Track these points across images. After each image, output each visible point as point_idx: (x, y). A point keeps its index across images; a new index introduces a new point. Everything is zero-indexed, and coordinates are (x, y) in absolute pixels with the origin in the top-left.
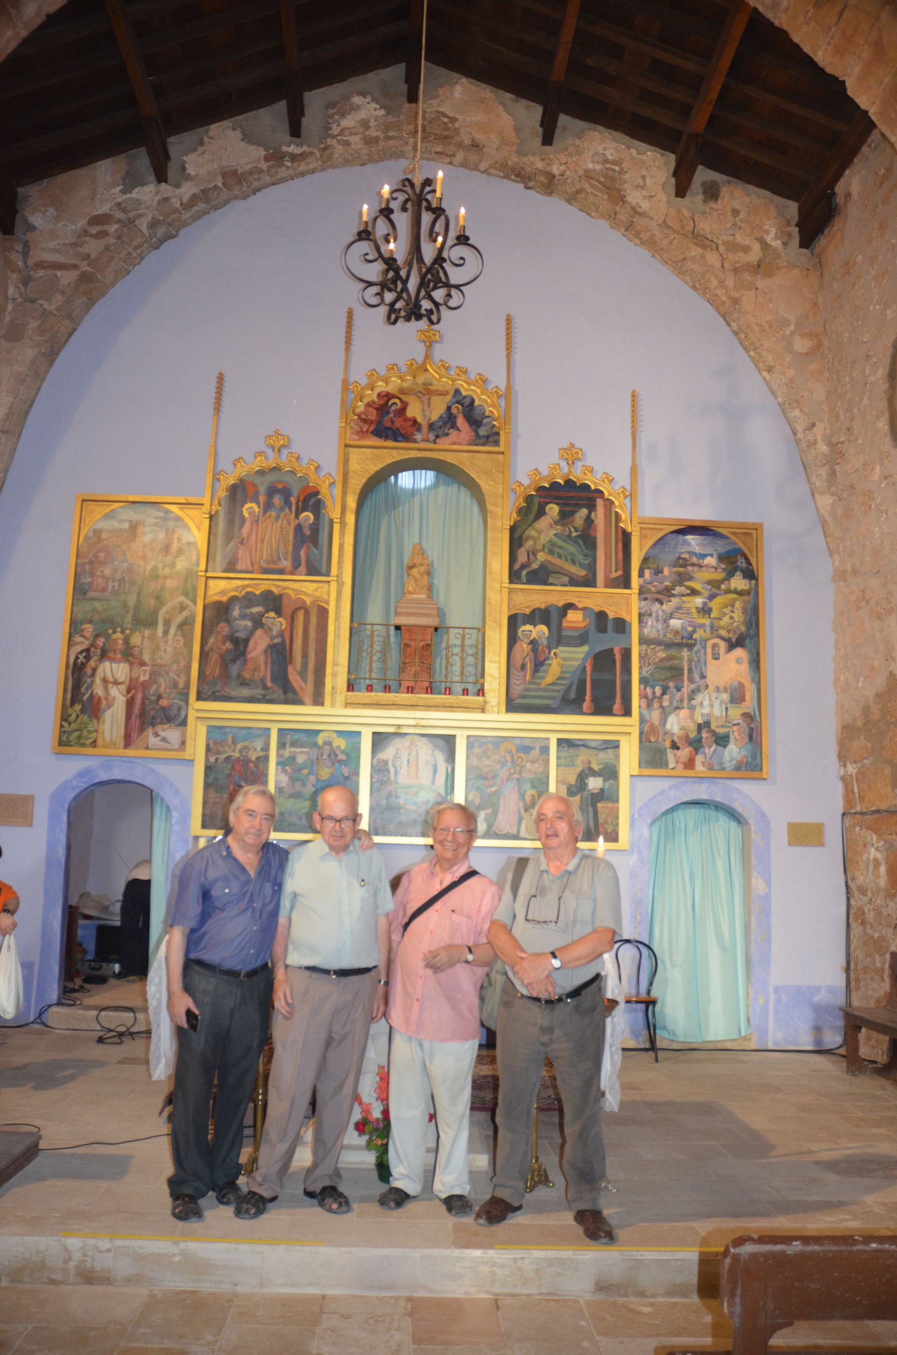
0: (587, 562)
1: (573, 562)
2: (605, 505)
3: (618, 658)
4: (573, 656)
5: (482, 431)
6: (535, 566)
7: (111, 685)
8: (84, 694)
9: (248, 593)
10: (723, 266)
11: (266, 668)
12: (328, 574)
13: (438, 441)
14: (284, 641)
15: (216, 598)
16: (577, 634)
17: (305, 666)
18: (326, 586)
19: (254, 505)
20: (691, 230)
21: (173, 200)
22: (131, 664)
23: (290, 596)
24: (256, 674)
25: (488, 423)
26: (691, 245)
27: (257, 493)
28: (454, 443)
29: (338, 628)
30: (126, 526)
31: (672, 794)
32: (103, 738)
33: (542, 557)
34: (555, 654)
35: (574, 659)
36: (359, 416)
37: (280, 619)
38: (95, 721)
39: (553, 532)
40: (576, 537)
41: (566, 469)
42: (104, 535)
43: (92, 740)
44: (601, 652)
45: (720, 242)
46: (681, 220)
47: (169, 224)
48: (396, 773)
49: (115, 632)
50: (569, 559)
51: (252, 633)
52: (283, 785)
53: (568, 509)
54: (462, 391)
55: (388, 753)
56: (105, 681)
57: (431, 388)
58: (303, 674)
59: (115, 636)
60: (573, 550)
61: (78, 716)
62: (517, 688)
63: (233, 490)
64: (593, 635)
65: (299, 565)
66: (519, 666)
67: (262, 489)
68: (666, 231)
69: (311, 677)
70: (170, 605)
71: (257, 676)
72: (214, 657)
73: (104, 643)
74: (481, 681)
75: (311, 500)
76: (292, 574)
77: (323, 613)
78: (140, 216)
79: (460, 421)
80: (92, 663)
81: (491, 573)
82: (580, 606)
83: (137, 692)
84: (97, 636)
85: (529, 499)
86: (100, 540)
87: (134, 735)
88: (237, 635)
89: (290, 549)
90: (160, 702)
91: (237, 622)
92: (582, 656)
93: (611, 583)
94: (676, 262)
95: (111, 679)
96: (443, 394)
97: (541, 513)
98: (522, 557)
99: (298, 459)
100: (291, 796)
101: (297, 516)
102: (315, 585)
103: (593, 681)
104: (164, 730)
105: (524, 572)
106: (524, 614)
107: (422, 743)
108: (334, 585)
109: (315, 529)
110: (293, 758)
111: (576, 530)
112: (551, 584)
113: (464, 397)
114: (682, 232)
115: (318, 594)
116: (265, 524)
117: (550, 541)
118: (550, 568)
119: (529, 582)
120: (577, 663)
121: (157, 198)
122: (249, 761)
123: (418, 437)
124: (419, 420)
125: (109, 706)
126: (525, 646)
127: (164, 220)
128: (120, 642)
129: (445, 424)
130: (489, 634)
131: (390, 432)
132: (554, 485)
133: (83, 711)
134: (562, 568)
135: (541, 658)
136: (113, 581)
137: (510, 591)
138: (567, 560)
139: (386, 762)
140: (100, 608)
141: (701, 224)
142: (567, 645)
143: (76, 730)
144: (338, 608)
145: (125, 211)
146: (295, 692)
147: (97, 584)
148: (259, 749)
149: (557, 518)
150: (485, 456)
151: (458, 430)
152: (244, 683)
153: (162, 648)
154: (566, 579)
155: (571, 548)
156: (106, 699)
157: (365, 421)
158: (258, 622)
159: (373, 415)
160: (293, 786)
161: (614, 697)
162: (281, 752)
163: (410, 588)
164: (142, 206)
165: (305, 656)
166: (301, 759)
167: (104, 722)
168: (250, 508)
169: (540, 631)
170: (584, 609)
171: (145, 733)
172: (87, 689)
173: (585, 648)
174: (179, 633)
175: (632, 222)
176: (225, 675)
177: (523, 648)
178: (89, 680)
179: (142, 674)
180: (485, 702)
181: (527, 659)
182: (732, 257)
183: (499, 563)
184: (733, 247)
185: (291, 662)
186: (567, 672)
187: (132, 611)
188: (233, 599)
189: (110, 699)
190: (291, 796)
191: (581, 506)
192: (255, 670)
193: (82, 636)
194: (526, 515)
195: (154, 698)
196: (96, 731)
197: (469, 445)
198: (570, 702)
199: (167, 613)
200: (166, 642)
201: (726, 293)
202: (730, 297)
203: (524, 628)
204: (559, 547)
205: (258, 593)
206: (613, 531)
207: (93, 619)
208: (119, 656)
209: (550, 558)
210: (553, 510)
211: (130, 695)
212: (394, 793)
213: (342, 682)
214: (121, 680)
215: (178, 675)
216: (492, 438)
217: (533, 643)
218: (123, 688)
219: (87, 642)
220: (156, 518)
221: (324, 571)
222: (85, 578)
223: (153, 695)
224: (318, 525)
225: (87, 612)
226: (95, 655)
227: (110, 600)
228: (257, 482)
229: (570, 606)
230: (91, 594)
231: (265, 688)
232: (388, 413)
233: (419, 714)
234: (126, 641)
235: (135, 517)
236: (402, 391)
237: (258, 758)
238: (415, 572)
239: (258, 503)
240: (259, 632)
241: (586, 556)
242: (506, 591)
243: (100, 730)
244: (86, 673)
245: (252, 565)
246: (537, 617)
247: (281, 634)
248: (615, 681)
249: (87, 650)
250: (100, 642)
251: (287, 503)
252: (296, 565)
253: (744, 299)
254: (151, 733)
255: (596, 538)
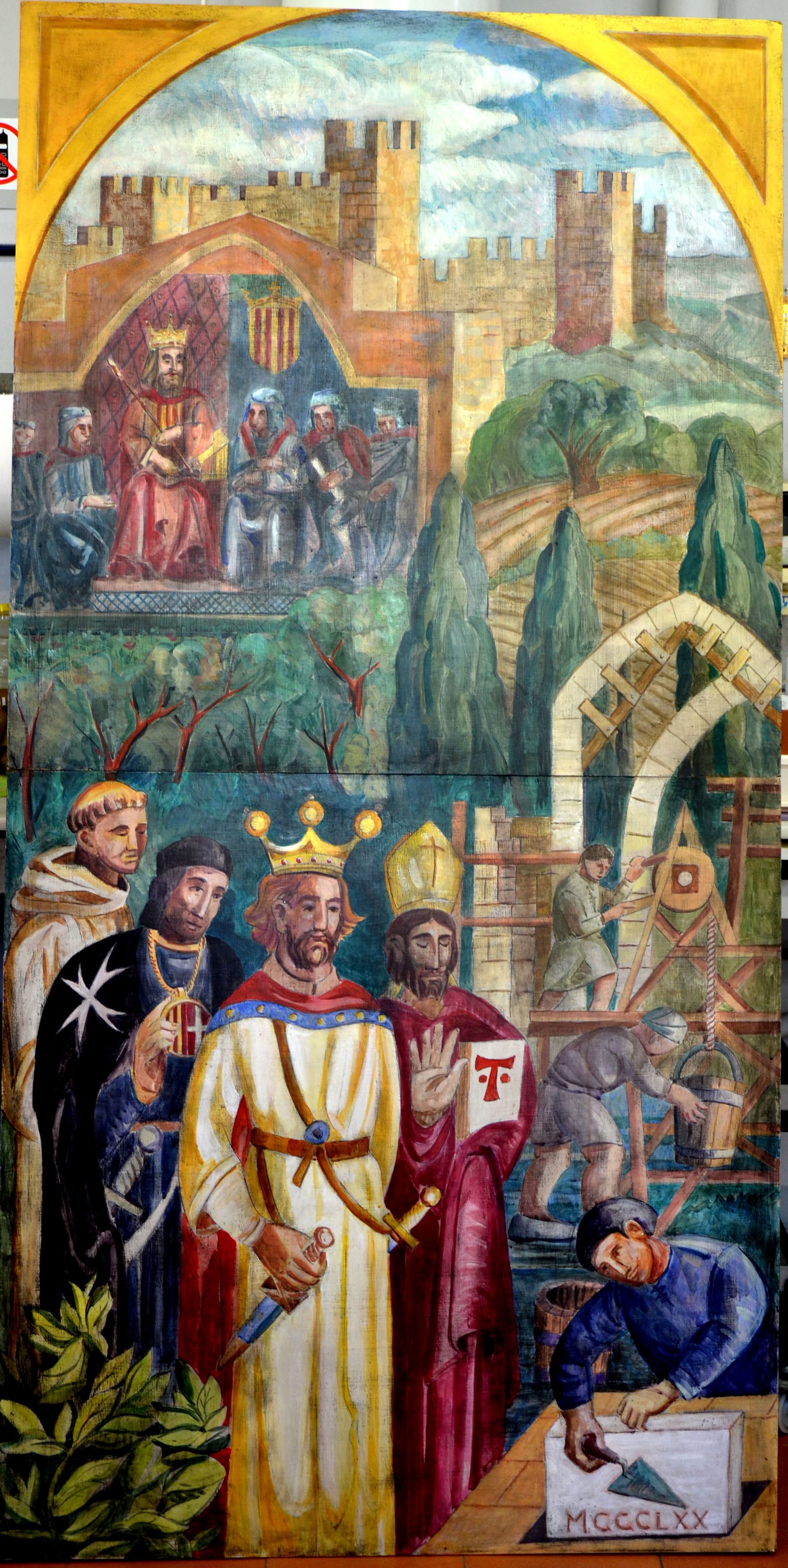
7: (292, 1163)
8: (126, 1226)
22: (407, 1029)
30: (305, 154)
32: (267, 1493)
38: (208, 1393)
42: (172, 219)
43: (196, 1506)
49: (287, 826)
56: (248, 1135)
59: (290, 855)
61: (94, 1362)
70: (620, 646)
73: (227, 899)
80: (160, 1030)
83: (452, 1199)
84: (174, 859)
86: (143, 239)
87: (455, 1460)
90: (602, 1255)
95: (291, 1127)
104: (634, 1424)
125: (290, 1294)
128: (327, 889)
133: (124, 1330)
136: (251, 509)
140: (180, 678)
143: (91, 1452)
147: (154, 530)
153: (593, 922)
156: (266, 1248)
167: (261, 1395)
171: (521, 1449)
172: (141, 1193)
174: (685, 821)
178: (149, 1136)
179: (477, 1090)
187: (380, 695)
189: (293, 1248)
193: (79, 858)
195: (560, 1230)
196: (218, 1449)
199: (600, 702)
200: (612, 878)
207: (144, 747)
208: (326, 979)
211: (414, 1218)
214: (349, 1133)
215: (699, 1085)
218: (367, 1177)
219: (119, 898)
220: (486, 104)
222: (71, 488)
223: (558, 1211)
225: (100, 710)
226: (177, 979)
227: (233, 631)
230: (117, 593)
234: (365, 884)
235: (356, 102)
243: (243, 1443)
244: (126, 1090)
249: (124, 948)
250: (202, 894)
254: (555, 1447)
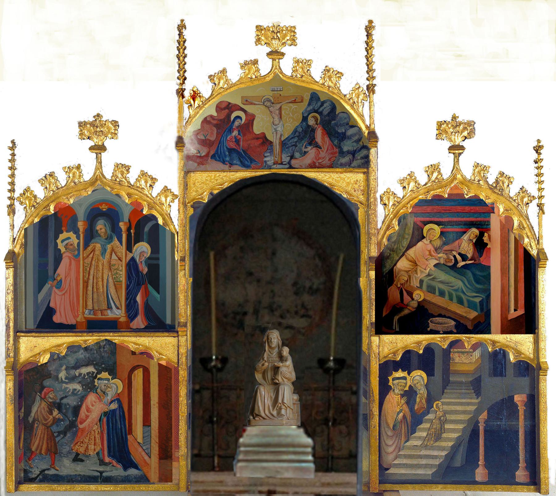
0: (477, 300)
1: (460, 301)
5: (347, 146)
14: (121, 406)
51: (83, 399)
72: (39, 431)
79: (319, 135)
124: (270, 137)
129: (301, 139)
154: (453, 323)
185: (130, 432)
232: (231, 131)
240: (91, 398)
247: (118, 399)
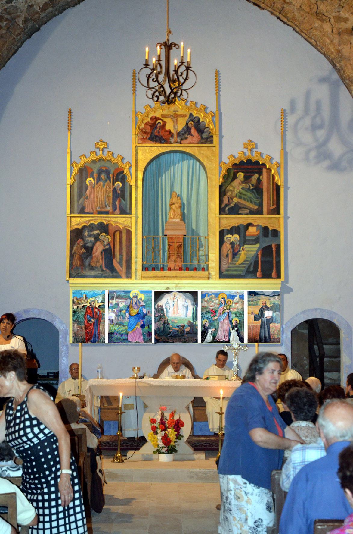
0: (258, 202)
1: (251, 202)
2: (267, 172)
3: (274, 249)
4: (252, 249)
5: (204, 136)
6: (232, 205)
9: (91, 224)
10: (332, 32)
11: (102, 261)
12: (130, 213)
13: (182, 142)
14: (110, 247)
15: (76, 227)
16: (253, 238)
17: (121, 259)
18: (129, 219)
19: (91, 179)
20: (316, 10)
21: (35, 6)
23: (112, 225)
24: (98, 264)
25: (207, 131)
26: (315, 20)
27: (93, 173)
28: (190, 143)
29: (136, 240)
31: (302, 316)
33: (235, 200)
34: (243, 249)
35: (252, 251)
36: (141, 130)
37: (108, 236)
39: (241, 187)
40: (253, 189)
41: (248, 153)
44: (266, 247)
45: (332, 17)
46: (310, 6)
47: (34, 21)
48: (167, 311)
50: (249, 200)
52: (113, 318)
53: (248, 175)
54: (194, 114)
55: (163, 302)
57: (178, 113)
58: (120, 263)
60: (251, 196)
62: (224, 266)
63: (81, 170)
64: (262, 239)
65: (116, 209)
66: (225, 255)
67: (95, 171)
68: (301, 12)
69: (124, 265)
71: (98, 265)
72: (77, 257)
74: (207, 263)
75: (120, 176)
76: (113, 214)
77: (129, 232)
78: (18, 16)
79: (193, 131)
81: (210, 209)
82: (255, 224)
85: (228, 170)
88: (87, 245)
89: (111, 201)
91: (87, 238)
92: (256, 249)
93: (271, 212)
94: (307, 31)
96: (184, 116)
97: (235, 177)
98: (226, 200)
99: (113, 154)
100: (117, 324)
101: (113, 184)
102: (124, 219)
103: (261, 262)
105: (227, 208)
106: (227, 230)
107: (180, 295)
108: (133, 215)
109: (123, 190)
110: (118, 305)
111: (253, 185)
112: (240, 214)
113: (195, 118)
114: (310, 12)
115: (126, 223)
116: (98, 189)
117: (239, 192)
118: (240, 205)
119: (229, 214)
120: (254, 253)
121: (26, 5)
122: (95, 307)
123: (172, 140)
124: (172, 131)
126: (228, 245)
127: (31, 19)
129: (185, 133)
130: (210, 239)
131: (157, 138)
132: (242, 162)
134: (246, 205)
135: (236, 251)
137: (220, 218)
138: (248, 201)
139: (162, 306)
141: (321, 7)
142: (249, 244)
144: (136, 230)
145: (9, 14)
146: (117, 272)
148: (100, 301)
149: (243, 180)
150: (206, 148)
151: (192, 135)
152: (92, 268)
154: (248, 211)
155: (250, 195)
157: (145, 133)
158: (97, 238)
159: (149, 129)
160: (118, 319)
161: (273, 269)
162: (111, 301)
163: (172, 216)
164: (19, 10)
165: (121, 254)
166: (121, 305)
168: (90, 181)
169: (235, 238)
170: (257, 226)
173: (258, 245)
175: (283, 7)
176: (82, 264)
177: (227, 247)
180: (209, 274)
181: (229, 252)
182: (337, 26)
183: (215, 204)
184: (339, 19)
185: (114, 257)
186: (249, 258)
188: (84, 227)
190: (117, 324)
191: (255, 173)
192: (97, 262)
194: (227, 179)
197: (198, 143)
198: (250, 272)
201: (334, 47)
202: (336, 50)
203: (227, 236)
204: (244, 195)
205: (96, 224)
206: (271, 185)
209: (239, 201)
210: (241, 175)
212: (166, 322)
213: (140, 267)
216: (209, 140)
217: (232, 244)
221: (128, 211)
224: (124, 188)
228: (92, 167)
229: (250, 224)
231: (102, 270)
232: (156, 128)
233: (177, 282)
236: (163, 116)
237: (99, 306)
238: (174, 206)
239: (94, 178)
240: (98, 243)
241: (257, 198)
242: (218, 218)
245: (93, 210)
246: (234, 230)
247: (109, 244)
248: (272, 262)
251: (108, 177)
252: (114, 209)
253: (344, 50)
255: (262, 189)
